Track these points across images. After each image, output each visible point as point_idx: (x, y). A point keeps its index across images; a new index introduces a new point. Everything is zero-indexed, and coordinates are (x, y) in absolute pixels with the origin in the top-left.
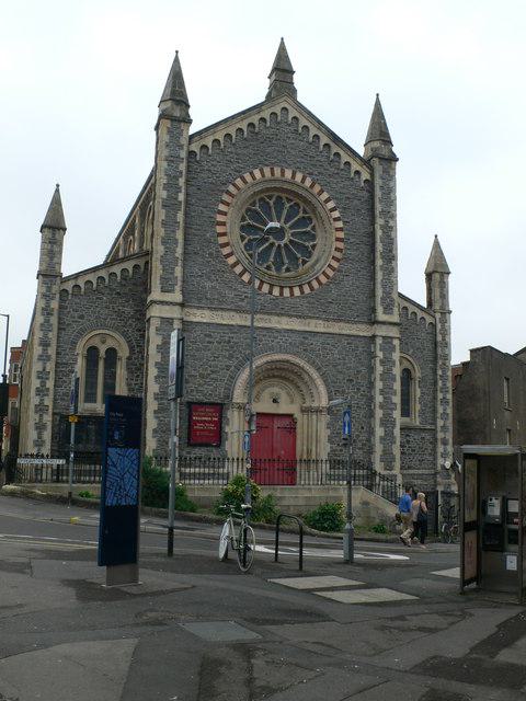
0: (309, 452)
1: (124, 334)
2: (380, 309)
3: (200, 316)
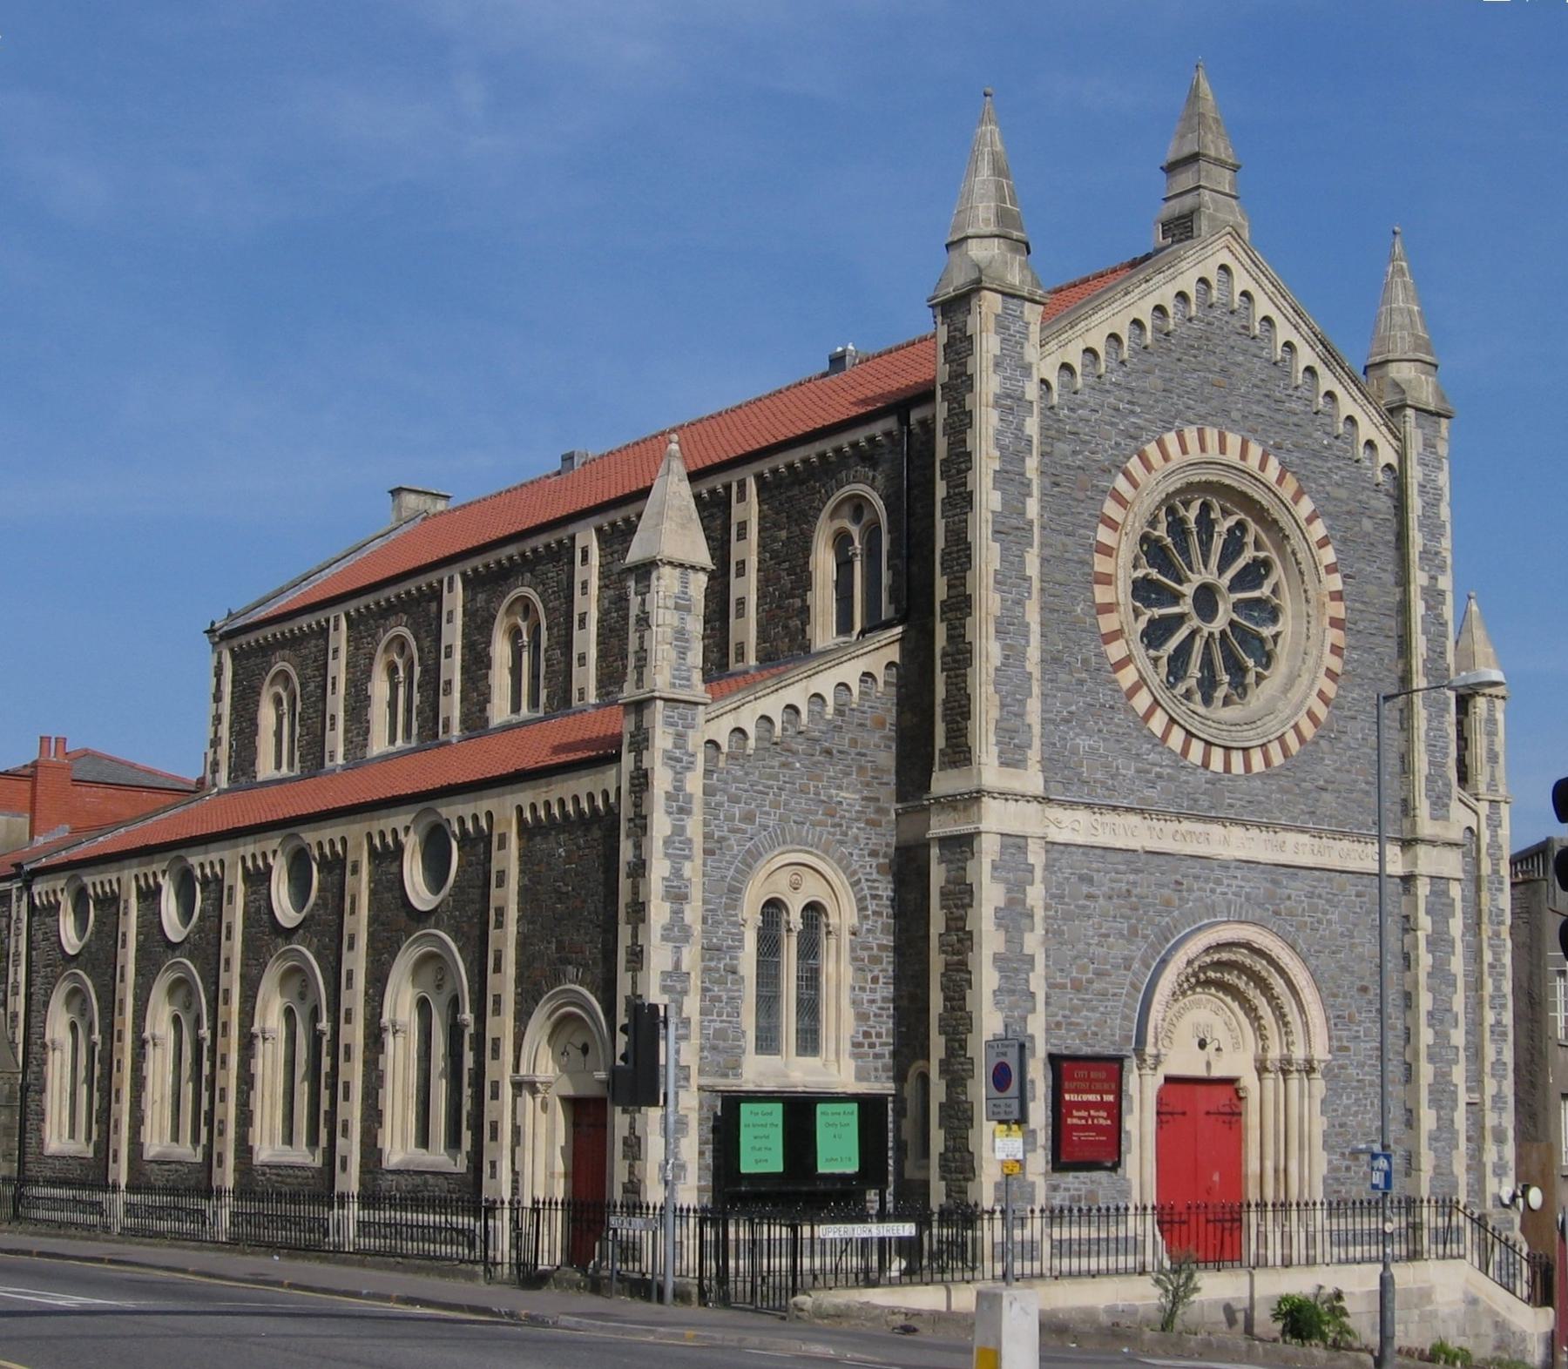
0: (1282, 1174)
1: (844, 864)
2: (1423, 807)
3: (1074, 826)
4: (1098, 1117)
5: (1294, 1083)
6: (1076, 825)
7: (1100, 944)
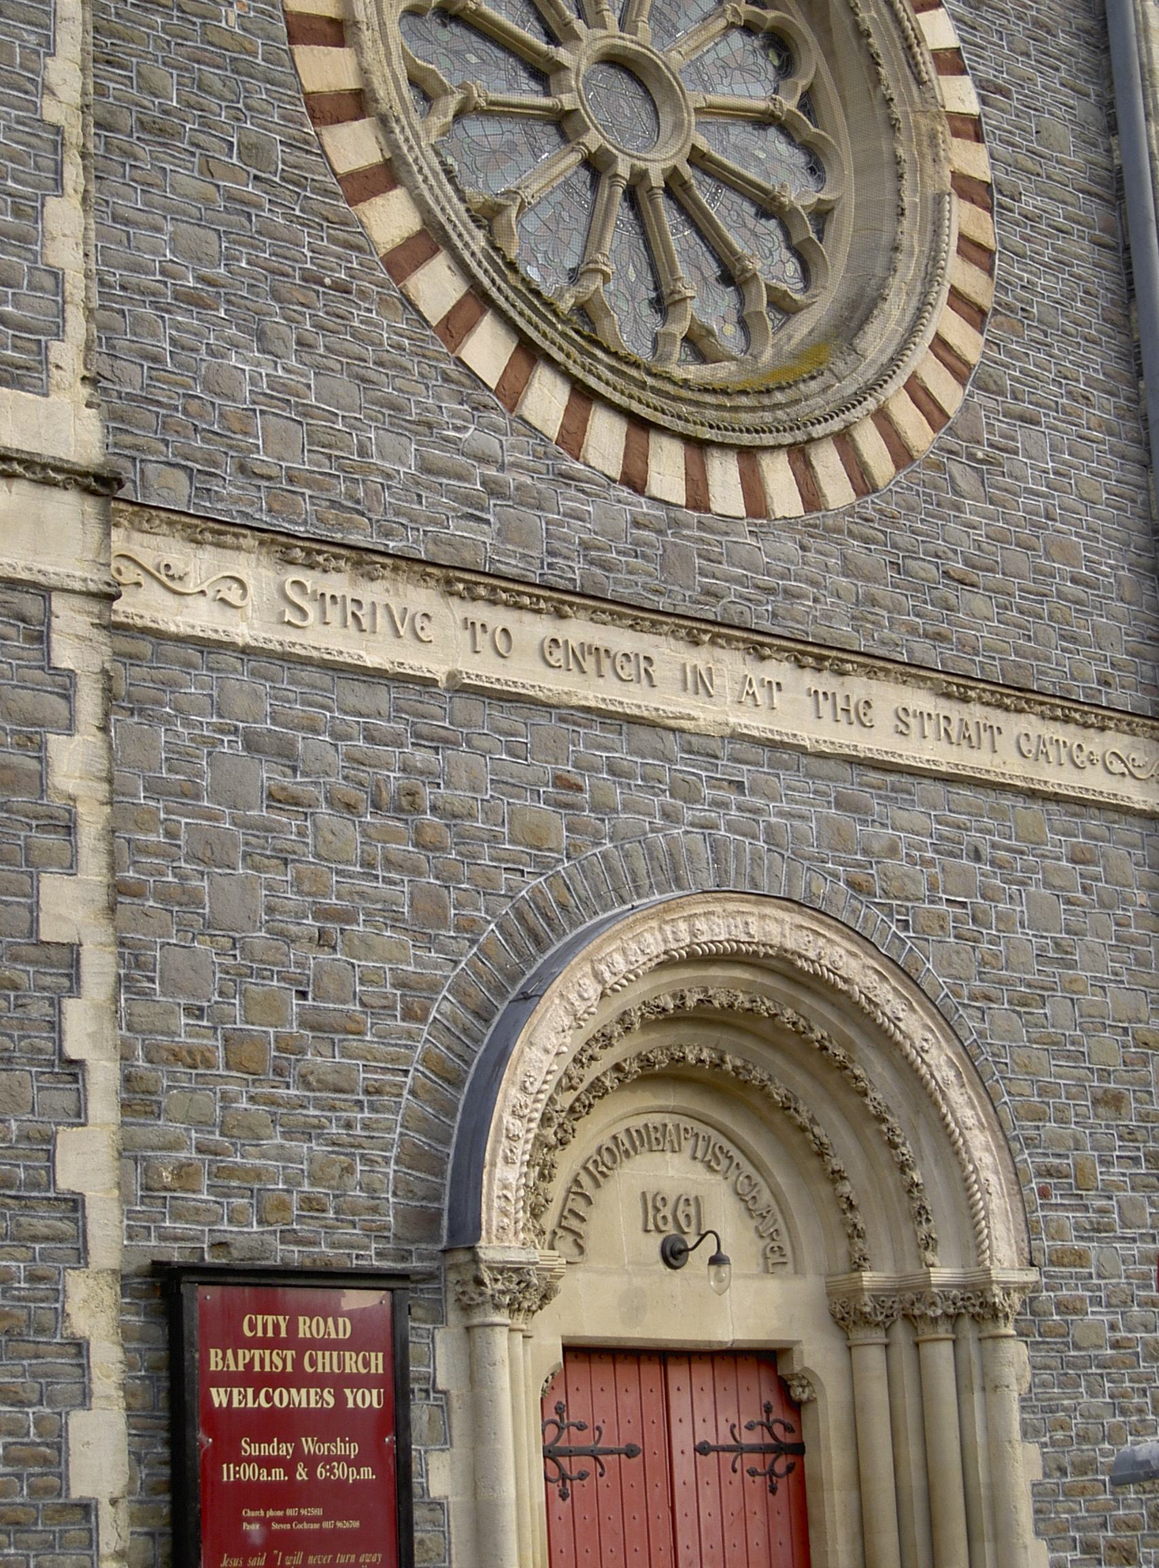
4: (329, 1459)
5: (941, 1355)
6: (233, 595)
7: (323, 940)
